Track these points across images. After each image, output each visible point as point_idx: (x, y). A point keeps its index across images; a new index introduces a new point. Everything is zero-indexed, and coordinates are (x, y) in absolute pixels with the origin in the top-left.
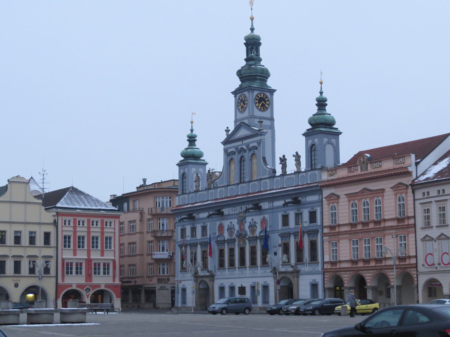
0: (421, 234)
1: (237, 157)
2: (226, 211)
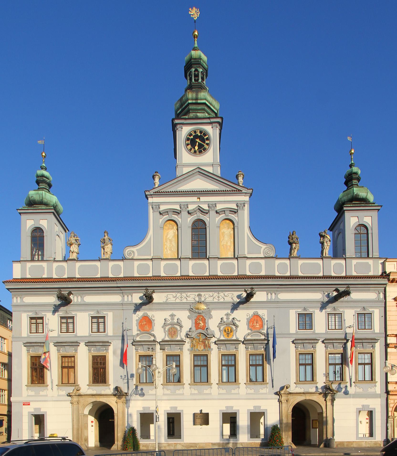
2: (158, 297)
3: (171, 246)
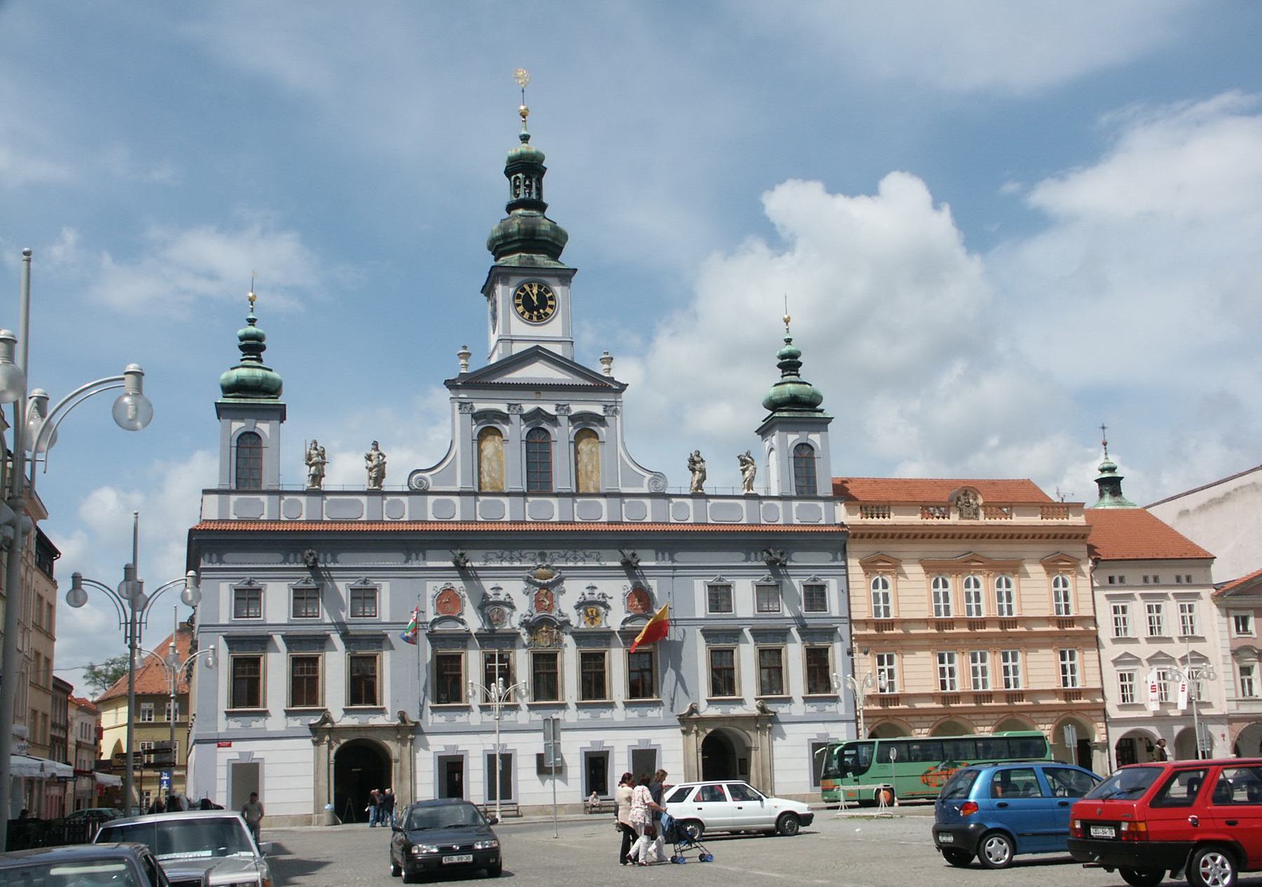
0: (1111, 651)
1: (515, 431)
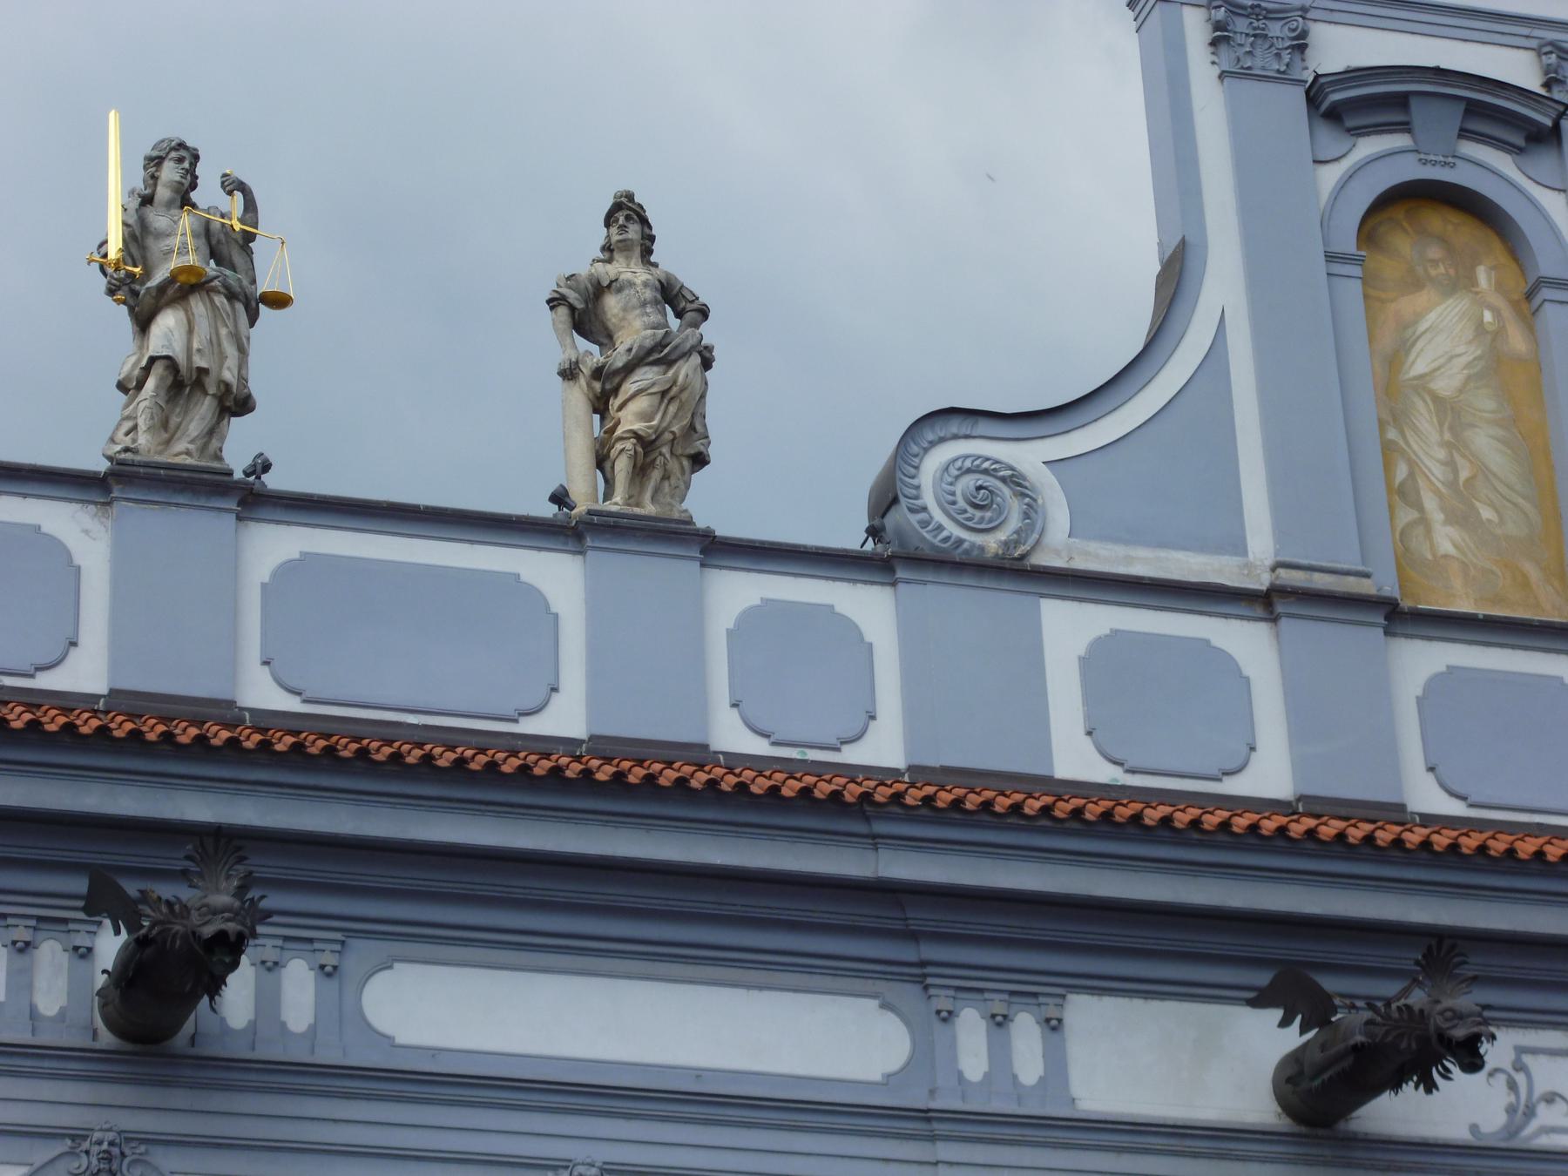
3: (1464, 474)
